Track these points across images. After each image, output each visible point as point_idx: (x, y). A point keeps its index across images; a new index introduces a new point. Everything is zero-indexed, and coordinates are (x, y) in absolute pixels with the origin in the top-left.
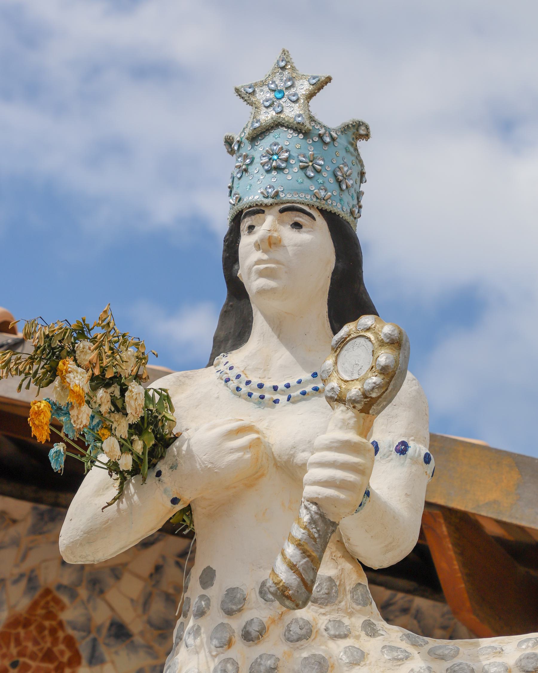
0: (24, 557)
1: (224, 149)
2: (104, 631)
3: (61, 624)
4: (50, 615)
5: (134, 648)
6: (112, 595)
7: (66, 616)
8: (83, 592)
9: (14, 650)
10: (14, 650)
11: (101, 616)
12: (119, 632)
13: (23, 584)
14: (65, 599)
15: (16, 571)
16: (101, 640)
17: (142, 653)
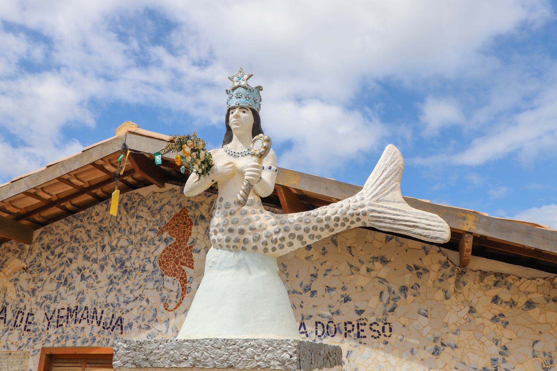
1: (226, 93)
4: (185, 214)
6: (200, 209)
7: (189, 214)
8: (193, 208)
9: (176, 222)
10: (176, 222)
11: (198, 214)
13: (178, 206)
14: (189, 210)
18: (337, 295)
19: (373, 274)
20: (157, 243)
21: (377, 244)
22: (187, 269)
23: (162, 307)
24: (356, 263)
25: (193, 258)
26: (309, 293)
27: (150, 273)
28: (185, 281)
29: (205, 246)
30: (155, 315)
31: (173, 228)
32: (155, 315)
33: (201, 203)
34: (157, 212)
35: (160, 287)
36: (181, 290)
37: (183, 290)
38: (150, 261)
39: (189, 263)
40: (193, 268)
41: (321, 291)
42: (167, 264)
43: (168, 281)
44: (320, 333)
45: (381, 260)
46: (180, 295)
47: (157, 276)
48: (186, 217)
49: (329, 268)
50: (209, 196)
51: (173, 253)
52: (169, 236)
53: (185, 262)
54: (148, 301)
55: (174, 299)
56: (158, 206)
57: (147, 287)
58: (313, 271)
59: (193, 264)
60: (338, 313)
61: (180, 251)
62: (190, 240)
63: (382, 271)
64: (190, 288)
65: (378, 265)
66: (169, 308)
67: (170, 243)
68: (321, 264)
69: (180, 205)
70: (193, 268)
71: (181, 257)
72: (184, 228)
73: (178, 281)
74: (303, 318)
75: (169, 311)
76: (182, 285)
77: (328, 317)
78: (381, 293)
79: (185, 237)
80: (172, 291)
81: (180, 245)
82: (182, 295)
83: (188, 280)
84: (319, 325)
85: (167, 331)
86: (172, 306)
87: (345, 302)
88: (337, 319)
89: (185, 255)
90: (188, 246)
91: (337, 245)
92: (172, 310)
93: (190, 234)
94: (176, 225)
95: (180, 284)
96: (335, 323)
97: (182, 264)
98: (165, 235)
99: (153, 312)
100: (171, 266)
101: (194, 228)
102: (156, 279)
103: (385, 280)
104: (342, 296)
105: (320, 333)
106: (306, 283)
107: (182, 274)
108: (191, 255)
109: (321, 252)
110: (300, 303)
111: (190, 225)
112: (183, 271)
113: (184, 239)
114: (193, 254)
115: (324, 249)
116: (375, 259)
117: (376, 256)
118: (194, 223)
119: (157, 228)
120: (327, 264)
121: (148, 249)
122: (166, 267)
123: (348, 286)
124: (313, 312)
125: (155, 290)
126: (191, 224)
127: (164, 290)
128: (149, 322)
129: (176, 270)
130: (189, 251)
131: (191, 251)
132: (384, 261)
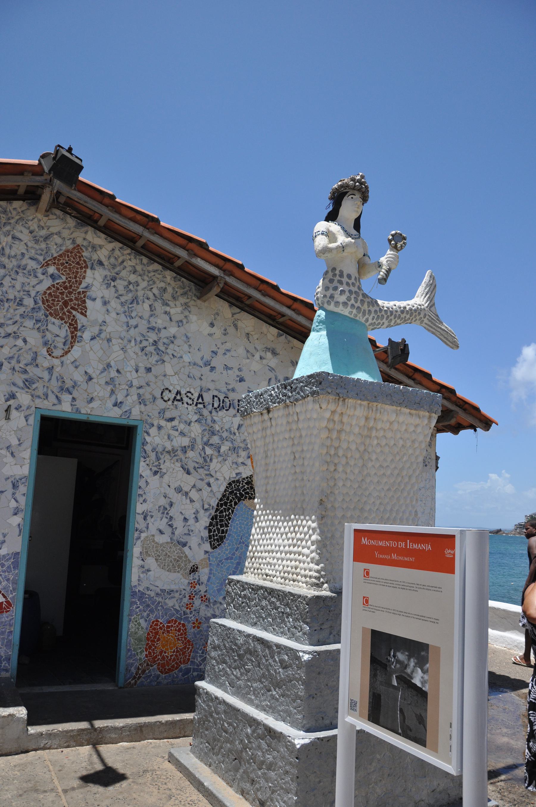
0: (72, 234)
2: (96, 262)
3: (82, 255)
4: (79, 252)
5: (105, 269)
6: (98, 252)
7: (84, 254)
8: (90, 249)
9: (67, 259)
10: (67, 259)
11: (95, 257)
12: (101, 263)
13: (71, 241)
14: (84, 249)
15: (69, 237)
16: (95, 264)
17: (107, 271)
18: (233, 374)
19: (264, 361)
20: (41, 277)
21: (270, 337)
22: (79, 316)
23: (44, 351)
24: (252, 350)
25: (86, 305)
26: (209, 368)
27: (29, 309)
28: (76, 329)
29: (102, 295)
30: (34, 359)
31: (62, 264)
32: (34, 359)
33: (101, 247)
34: (42, 239)
35: (42, 328)
36: (70, 335)
37: (72, 337)
38: (30, 295)
39: (81, 309)
40: (86, 316)
41: (220, 368)
42: (53, 304)
43: (54, 323)
44: (216, 405)
45: (272, 351)
46: (69, 342)
47: (40, 315)
48: (80, 257)
49: (228, 348)
50: (110, 242)
51: (62, 293)
52: (56, 272)
53: (76, 307)
54: (25, 341)
55: (60, 345)
56: (43, 233)
57: (24, 325)
58: (215, 349)
59: (86, 312)
60: (233, 390)
61: (70, 293)
62: (83, 285)
63: (273, 362)
64: (82, 337)
65: (269, 355)
66: (53, 355)
67: (58, 281)
68: (222, 344)
69: (74, 242)
70: (86, 316)
71: (71, 300)
72: (77, 269)
73: (66, 326)
74: (201, 390)
75: (53, 357)
76: (72, 333)
77: (225, 393)
78: (270, 379)
79: (78, 279)
80: (58, 336)
81: (71, 286)
82: (71, 343)
83: (79, 327)
84: (216, 398)
85: (50, 379)
86: (58, 352)
87: (240, 382)
88: (232, 395)
89: (76, 299)
90: (80, 290)
91: (237, 329)
92: (57, 358)
93: (84, 278)
94: (67, 263)
95: (69, 330)
96: (230, 399)
97: (72, 308)
98: (52, 270)
99: (32, 354)
100: (58, 307)
101: (89, 271)
102: (38, 318)
103: (273, 369)
104: (238, 376)
105: (216, 405)
106: (207, 357)
107: (72, 320)
108: (84, 302)
109: (223, 332)
110: (199, 376)
111: (85, 267)
112: (74, 316)
113: (76, 281)
114: (87, 301)
115: (225, 330)
116: (267, 349)
117: (269, 347)
118: (89, 266)
119: (41, 258)
120: (227, 344)
121: (28, 281)
122: (51, 307)
123: (244, 368)
124: (211, 386)
125: (36, 331)
126: (86, 267)
127: (47, 332)
128: (27, 365)
129: (64, 313)
130: (82, 296)
131: (84, 297)
132: (274, 353)
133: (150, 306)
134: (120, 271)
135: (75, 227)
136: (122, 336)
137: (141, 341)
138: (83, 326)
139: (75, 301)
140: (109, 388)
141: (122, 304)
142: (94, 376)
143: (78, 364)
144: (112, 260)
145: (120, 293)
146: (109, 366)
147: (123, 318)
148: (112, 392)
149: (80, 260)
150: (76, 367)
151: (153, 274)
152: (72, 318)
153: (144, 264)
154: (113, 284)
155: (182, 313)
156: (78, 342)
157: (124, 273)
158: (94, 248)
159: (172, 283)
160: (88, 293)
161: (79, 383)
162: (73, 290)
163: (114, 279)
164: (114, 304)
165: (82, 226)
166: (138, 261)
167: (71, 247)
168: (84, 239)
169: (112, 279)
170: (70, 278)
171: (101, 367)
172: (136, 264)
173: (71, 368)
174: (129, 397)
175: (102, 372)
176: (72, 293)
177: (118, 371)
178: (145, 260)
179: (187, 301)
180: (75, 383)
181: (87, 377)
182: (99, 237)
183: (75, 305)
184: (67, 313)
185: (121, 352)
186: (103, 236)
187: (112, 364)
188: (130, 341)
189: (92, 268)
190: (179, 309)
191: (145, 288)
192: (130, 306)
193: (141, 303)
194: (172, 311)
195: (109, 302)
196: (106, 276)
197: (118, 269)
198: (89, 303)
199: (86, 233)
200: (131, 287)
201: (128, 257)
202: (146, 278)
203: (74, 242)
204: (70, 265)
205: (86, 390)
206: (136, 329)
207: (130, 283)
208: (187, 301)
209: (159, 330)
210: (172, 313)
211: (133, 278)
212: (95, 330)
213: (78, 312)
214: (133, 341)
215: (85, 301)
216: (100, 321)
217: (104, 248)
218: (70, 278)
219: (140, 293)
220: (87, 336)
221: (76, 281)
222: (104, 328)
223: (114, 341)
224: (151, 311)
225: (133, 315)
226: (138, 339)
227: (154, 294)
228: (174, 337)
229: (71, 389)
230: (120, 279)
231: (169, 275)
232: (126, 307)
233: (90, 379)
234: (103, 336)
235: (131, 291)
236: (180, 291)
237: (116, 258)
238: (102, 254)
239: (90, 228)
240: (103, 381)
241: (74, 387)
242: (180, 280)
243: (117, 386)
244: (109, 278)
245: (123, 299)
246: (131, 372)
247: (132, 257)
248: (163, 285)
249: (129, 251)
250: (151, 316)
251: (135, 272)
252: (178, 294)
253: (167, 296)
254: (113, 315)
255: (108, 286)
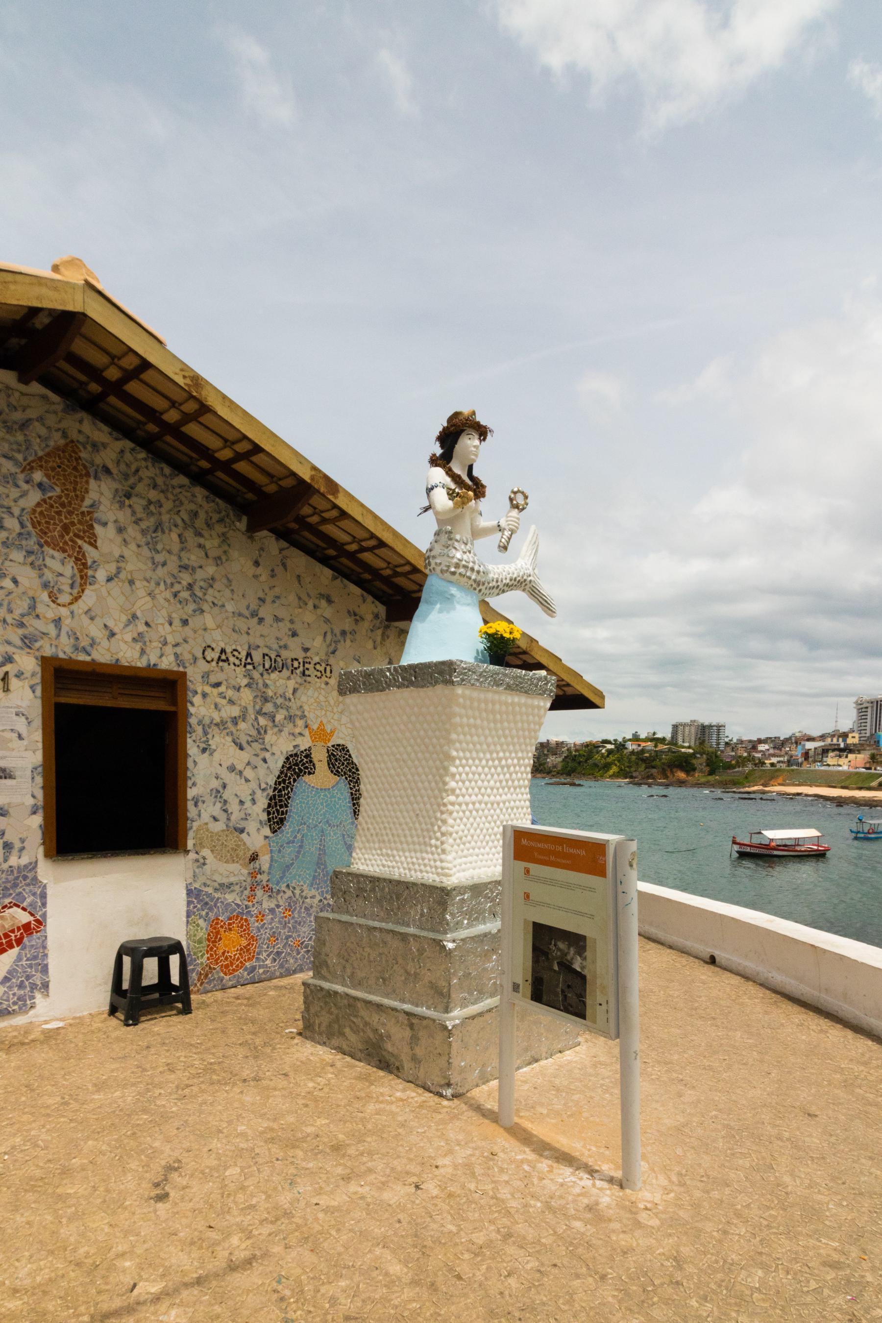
0: (60, 421)
5: (114, 479)
8: (89, 448)
12: (107, 471)
22: (86, 547)
28: (85, 565)
33: (105, 446)
36: (78, 576)
37: (82, 577)
39: (89, 537)
40: (96, 547)
48: (76, 459)
50: (117, 439)
53: (81, 534)
59: (95, 541)
62: (87, 502)
64: (94, 577)
70: (96, 547)
71: (73, 524)
76: (81, 571)
81: (70, 503)
82: (81, 585)
83: (89, 563)
90: (84, 509)
93: (87, 491)
94: (59, 467)
101: (93, 483)
108: (91, 527)
112: (80, 547)
114: (95, 525)
126: (88, 475)
130: (88, 518)
131: (91, 519)
133: (179, 536)
134: (135, 484)
135: (64, 411)
136: (148, 577)
137: (172, 584)
138: (95, 562)
139: (78, 526)
140: (138, 646)
141: (144, 532)
142: (116, 630)
143: (93, 614)
144: (123, 467)
145: (139, 516)
146: (134, 617)
147: (145, 551)
148: (143, 652)
149: (78, 463)
150: (92, 619)
151: (179, 490)
152: (77, 549)
153: (165, 475)
154: (127, 502)
155: (220, 546)
156: (90, 584)
157: (140, 488)
158: (96, 447)
159: (204, 504)
160: (95, 515)
161: (98, 641)
162: (74, 508)
163: (128, 496)
164: (132, 532)
165: (73, 410)
166: (158, 472)
167: (62, 442)
168: (80, 432)
169: (125, 496)
170: (67, 490)
171: (124, 618)
172: (156, 475)
173: (86, 620)
174: (164, 658)
175: (127, 626)
176: (73, 513)
177: (147, 624)
178: (167, 470)
179: (225, 530)
180: (93, 640)
181: (107, 633)
182: (100, 430)
183: (80, 530)
184: (70, 543)
185: (148, 599)
186: (106, 429)
187: (139, 614)
188: (158, 584)
189: (96, 478)
190: (216, 542)
191: (170, 510)
192: (154, 535)
193: (167, 531)
194: (208, 544)
195: (125, 528)
196: (117, 490)
197: (132, 480)
198: (98, 529)
199: (81, 422)
200: (152, 508)
201: (144, 464)
202: (170, 496)
203: (65, 435)
204: (64, 470)
205: (108, 650)
206: (165, 567)
207: (150, 502)
208: (225, 530)
209: (194, 569)
210: (207, 547)
211: (153, 495)
212: (112, 568)
213: (85, 541)
214: (162, 584)
215: (92, 526)
216: (117, 555)
217: (112, 449)
218: (67, 490)
219: (165, 518)
220: (101, 575)
221: (77, 496)
222: (122, 565)
223: (138, 583)
224: (182, 542)
225: (159, 547)
226: (169, 582)
227: (183, 520)
228: (213, 579)
229: (88, 648)
230: (137, 496)
231: (200, 492)
232: (149, 537)
233: (113, 634)
234: (122, 575)
235: (152, 514)
236: (216, 517)
237: (127, 465)
238: (107, 457)
239: (83, 414)
240: (128, 637)
241: (91, 645)
242: (214, 501)
243: (148, 643)
244: (121, 494)
245: (144, 525)
246: (163, 624)
247: (150, 464)
248: (193, 507)
249: (143, 455)
250: (182, 549)
251: (155, 486)
252: (214, 520)
253: (200, 523)
254: (133, 546)
255: (122, 505)
